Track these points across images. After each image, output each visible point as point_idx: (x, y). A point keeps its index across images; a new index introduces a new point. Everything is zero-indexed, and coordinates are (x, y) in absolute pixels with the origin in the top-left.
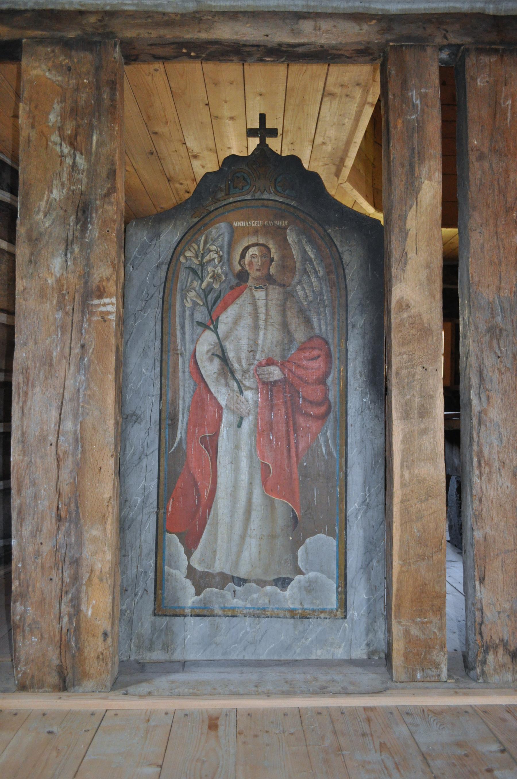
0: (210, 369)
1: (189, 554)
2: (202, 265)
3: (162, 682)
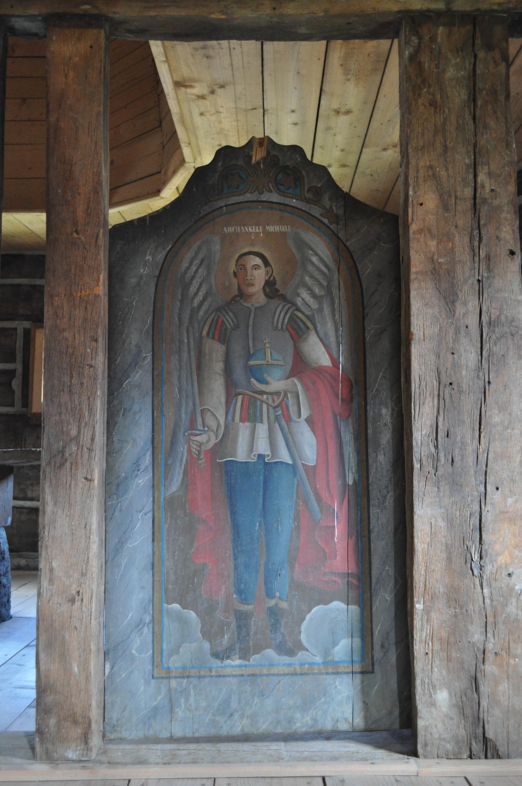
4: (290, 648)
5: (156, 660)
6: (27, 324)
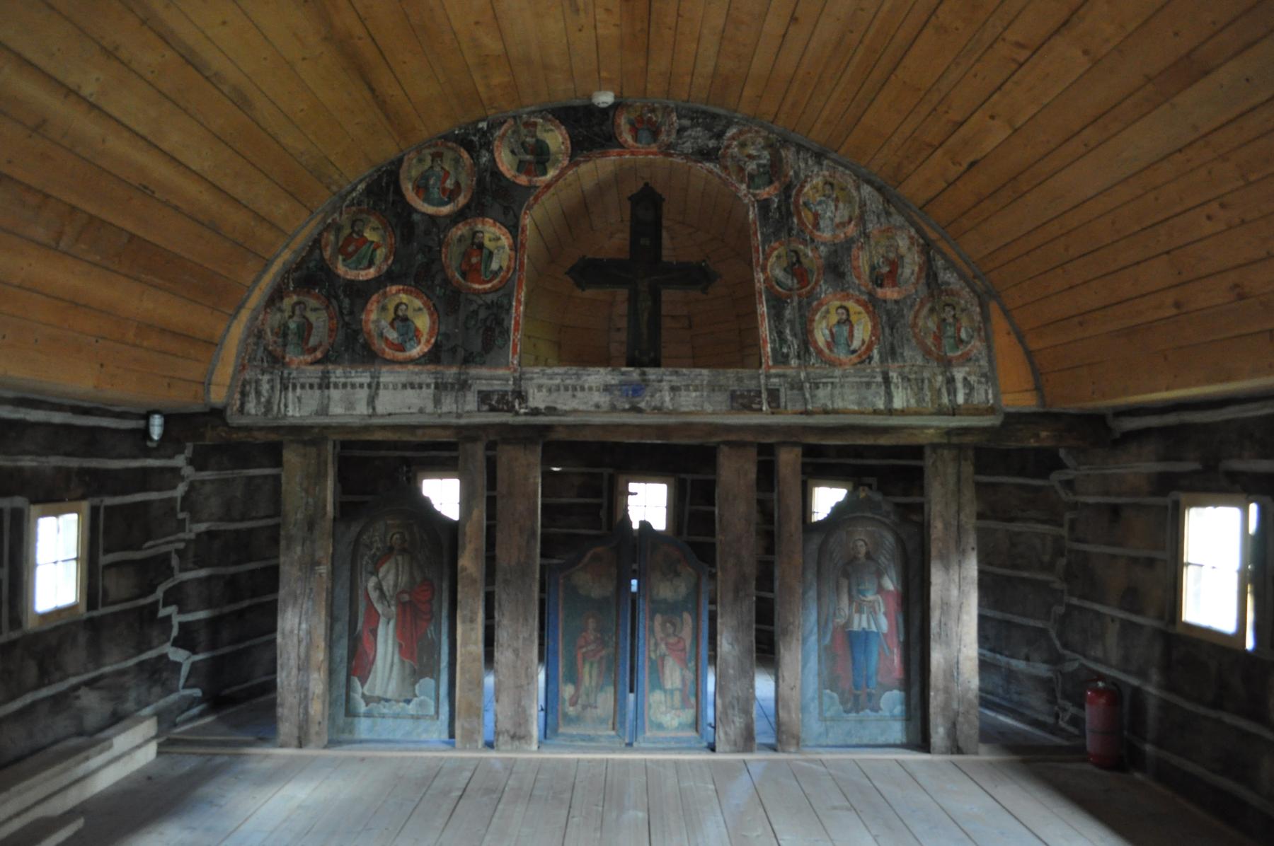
0: (374, 595)
1: (362, 686)
2: (372, 543)
3: (346, 747)
4: (876, 709)
5: (821, 712)
6: (611, 471)
